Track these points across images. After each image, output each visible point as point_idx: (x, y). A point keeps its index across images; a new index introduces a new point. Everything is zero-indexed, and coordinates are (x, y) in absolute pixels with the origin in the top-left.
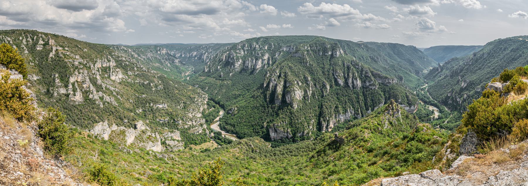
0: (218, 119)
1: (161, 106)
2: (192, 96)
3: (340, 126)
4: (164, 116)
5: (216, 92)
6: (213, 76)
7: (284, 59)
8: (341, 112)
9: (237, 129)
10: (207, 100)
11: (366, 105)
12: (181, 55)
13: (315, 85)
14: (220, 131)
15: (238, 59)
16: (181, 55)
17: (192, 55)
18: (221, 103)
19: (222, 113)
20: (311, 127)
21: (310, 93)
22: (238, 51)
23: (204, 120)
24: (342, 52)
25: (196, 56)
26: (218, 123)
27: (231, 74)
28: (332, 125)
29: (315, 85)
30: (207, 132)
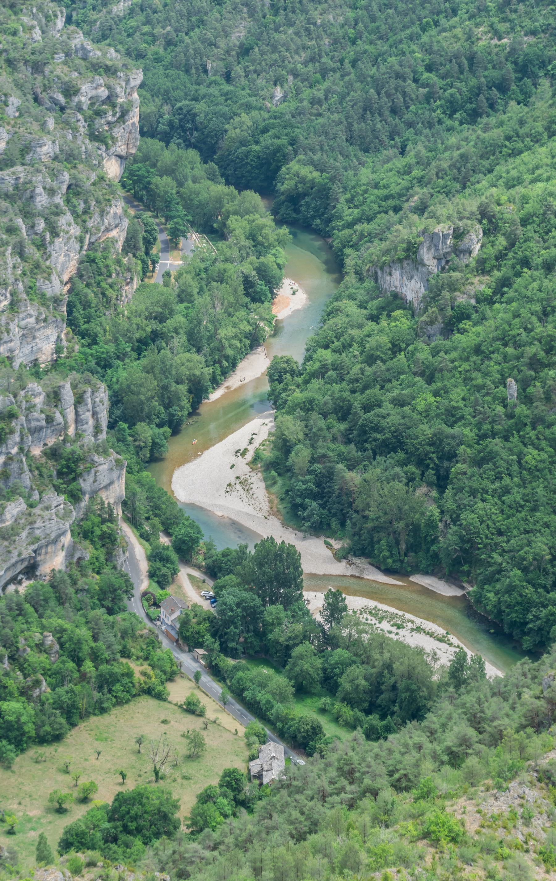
0: (253, 369)
5: (240, 33)
9: (482, 513)
18: (298, 171)
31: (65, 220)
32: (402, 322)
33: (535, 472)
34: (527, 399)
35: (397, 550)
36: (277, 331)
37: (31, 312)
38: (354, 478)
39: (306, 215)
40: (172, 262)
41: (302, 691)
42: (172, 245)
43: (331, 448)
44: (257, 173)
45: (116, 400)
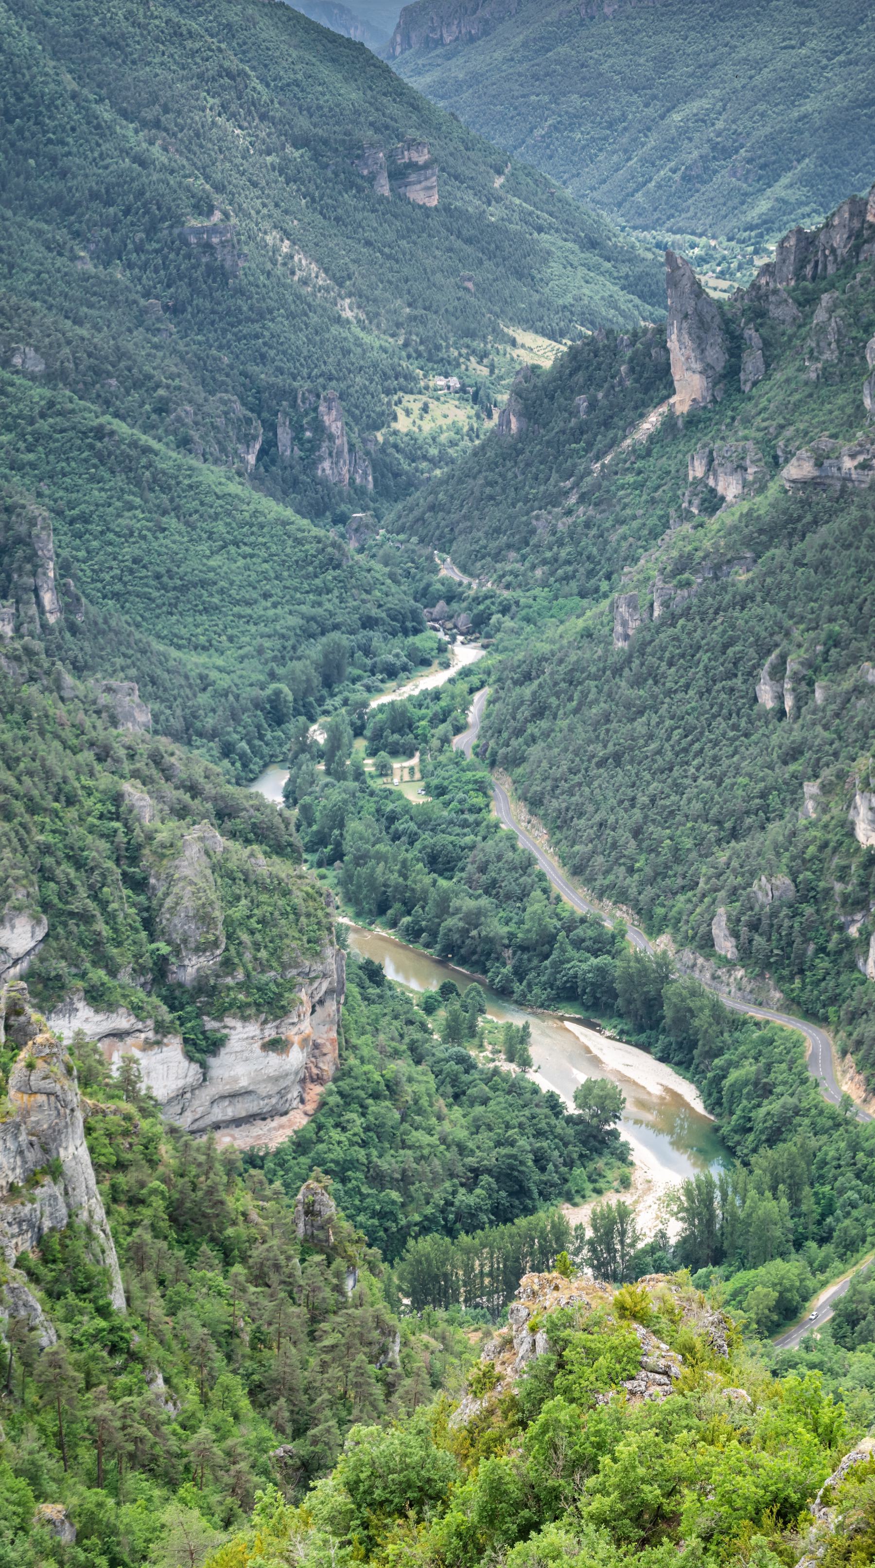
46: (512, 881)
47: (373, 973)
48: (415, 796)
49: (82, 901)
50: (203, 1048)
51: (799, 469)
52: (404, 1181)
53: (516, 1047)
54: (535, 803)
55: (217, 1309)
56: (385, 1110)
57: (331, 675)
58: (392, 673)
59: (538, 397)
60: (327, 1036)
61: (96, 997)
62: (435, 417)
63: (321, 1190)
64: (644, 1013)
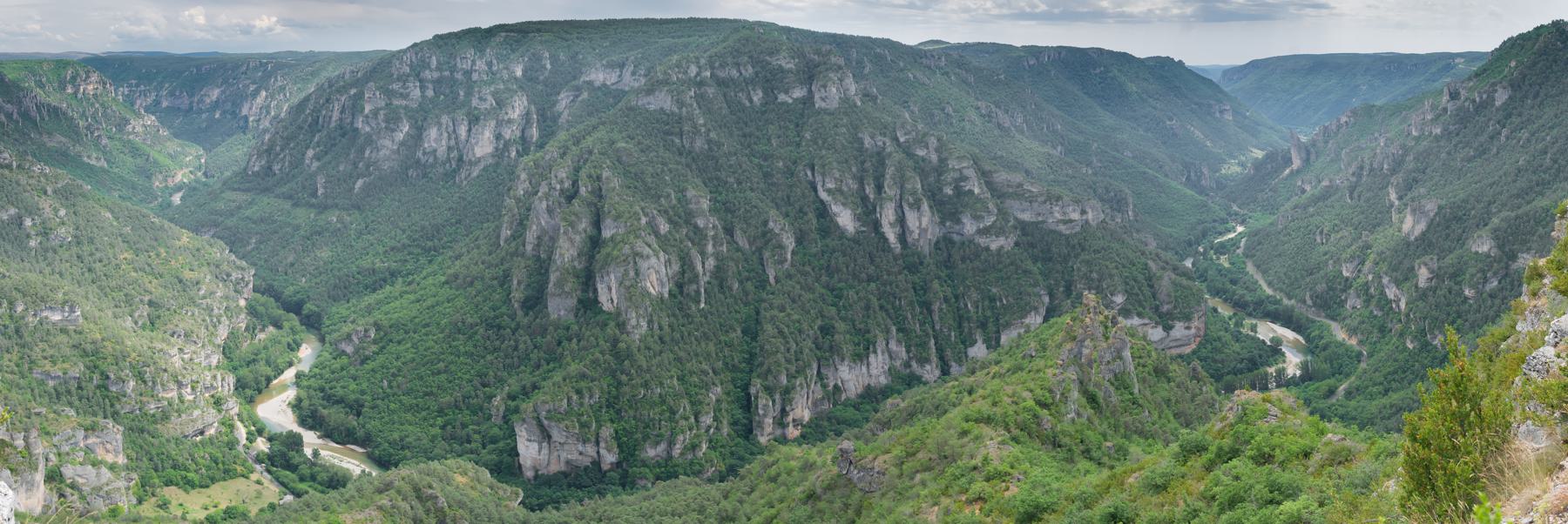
0: (290, 374)
1: (56, 317)
2: (187, 275)
3: (840, 412)
4: (65, 359)
5: (291, 259)
6: (284, 189)
7: (594, 121)
8: (847, 349)
10: (248, 292)
11: (960, 319)
12: (157, 103)
13: (729, 231)
14: (297, 429)
15: (393, 120)
16: (157, 103)
17: (201, 101)
18: (309, 307)
19: (307, 353)
20: (707, 420)
21: (704, 267)
22: (395, 86)
23: (231, 379)
24: (853, 88)
25: (216, 105)
26: (291, 394)
27: (359, 183)
28: (802, 411)
29: (729, 231)
30: (242, 432)
31: (224, 319)
32: (345, 360)
33: (394, 412)
34: (391, 387)
35: (341, 436)
36: (300, 361)
37: (209, 349)
38: (325, 412)
39: (312, 323)
40: (262, 336)
41: (302, 479)
42: (262, 330)
43: (316, 401)
44: (295, 307)
45: (238, 380)
46: (1253, 287)
47: (1215, 310)
48: (1227, 265)
49: (1136, 290)
50: (1168, 328)
51: (1325, 183)
52: (1222, 361)
53: (1254, 328)
54: (1258, 267)
55: (1165, 394)
56: (1218, 344)
57: (1204, 235)
58: (1221, 234)
59: (1258, 165)
60: (1202, 326)
61: (1140, 315)
62: (1232, 169)
63: (1196, 363)
64: (1288, 320)
